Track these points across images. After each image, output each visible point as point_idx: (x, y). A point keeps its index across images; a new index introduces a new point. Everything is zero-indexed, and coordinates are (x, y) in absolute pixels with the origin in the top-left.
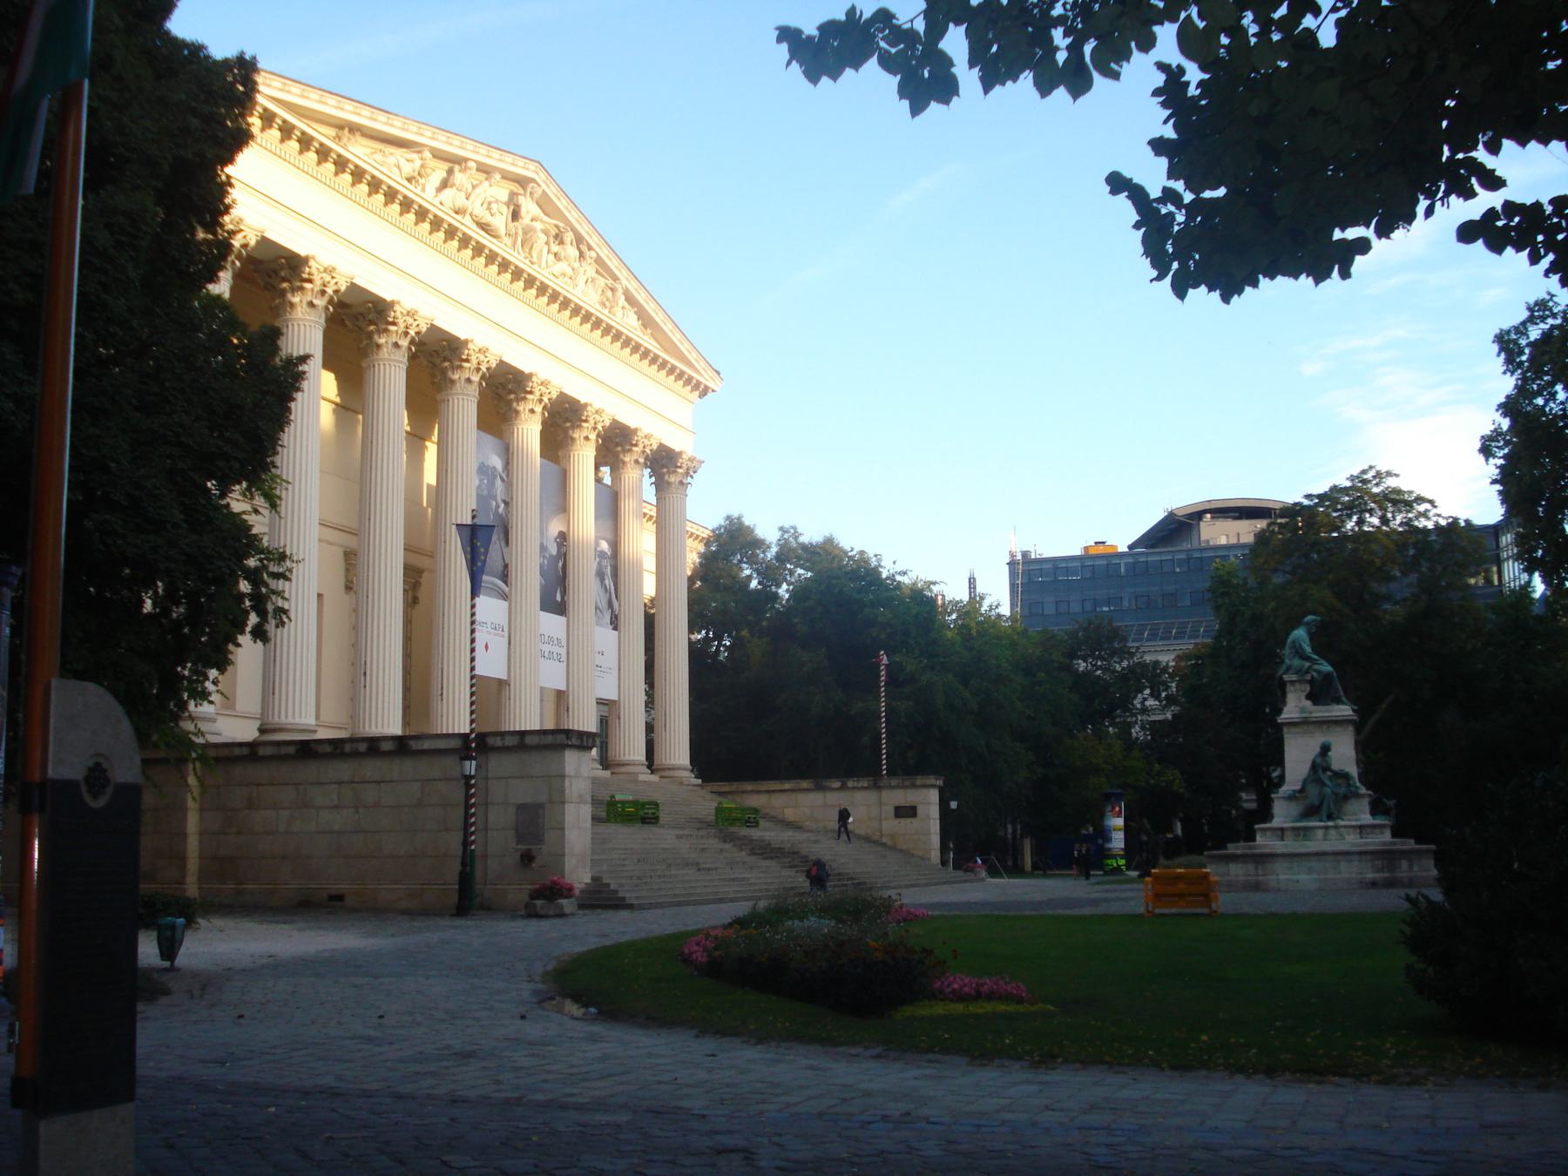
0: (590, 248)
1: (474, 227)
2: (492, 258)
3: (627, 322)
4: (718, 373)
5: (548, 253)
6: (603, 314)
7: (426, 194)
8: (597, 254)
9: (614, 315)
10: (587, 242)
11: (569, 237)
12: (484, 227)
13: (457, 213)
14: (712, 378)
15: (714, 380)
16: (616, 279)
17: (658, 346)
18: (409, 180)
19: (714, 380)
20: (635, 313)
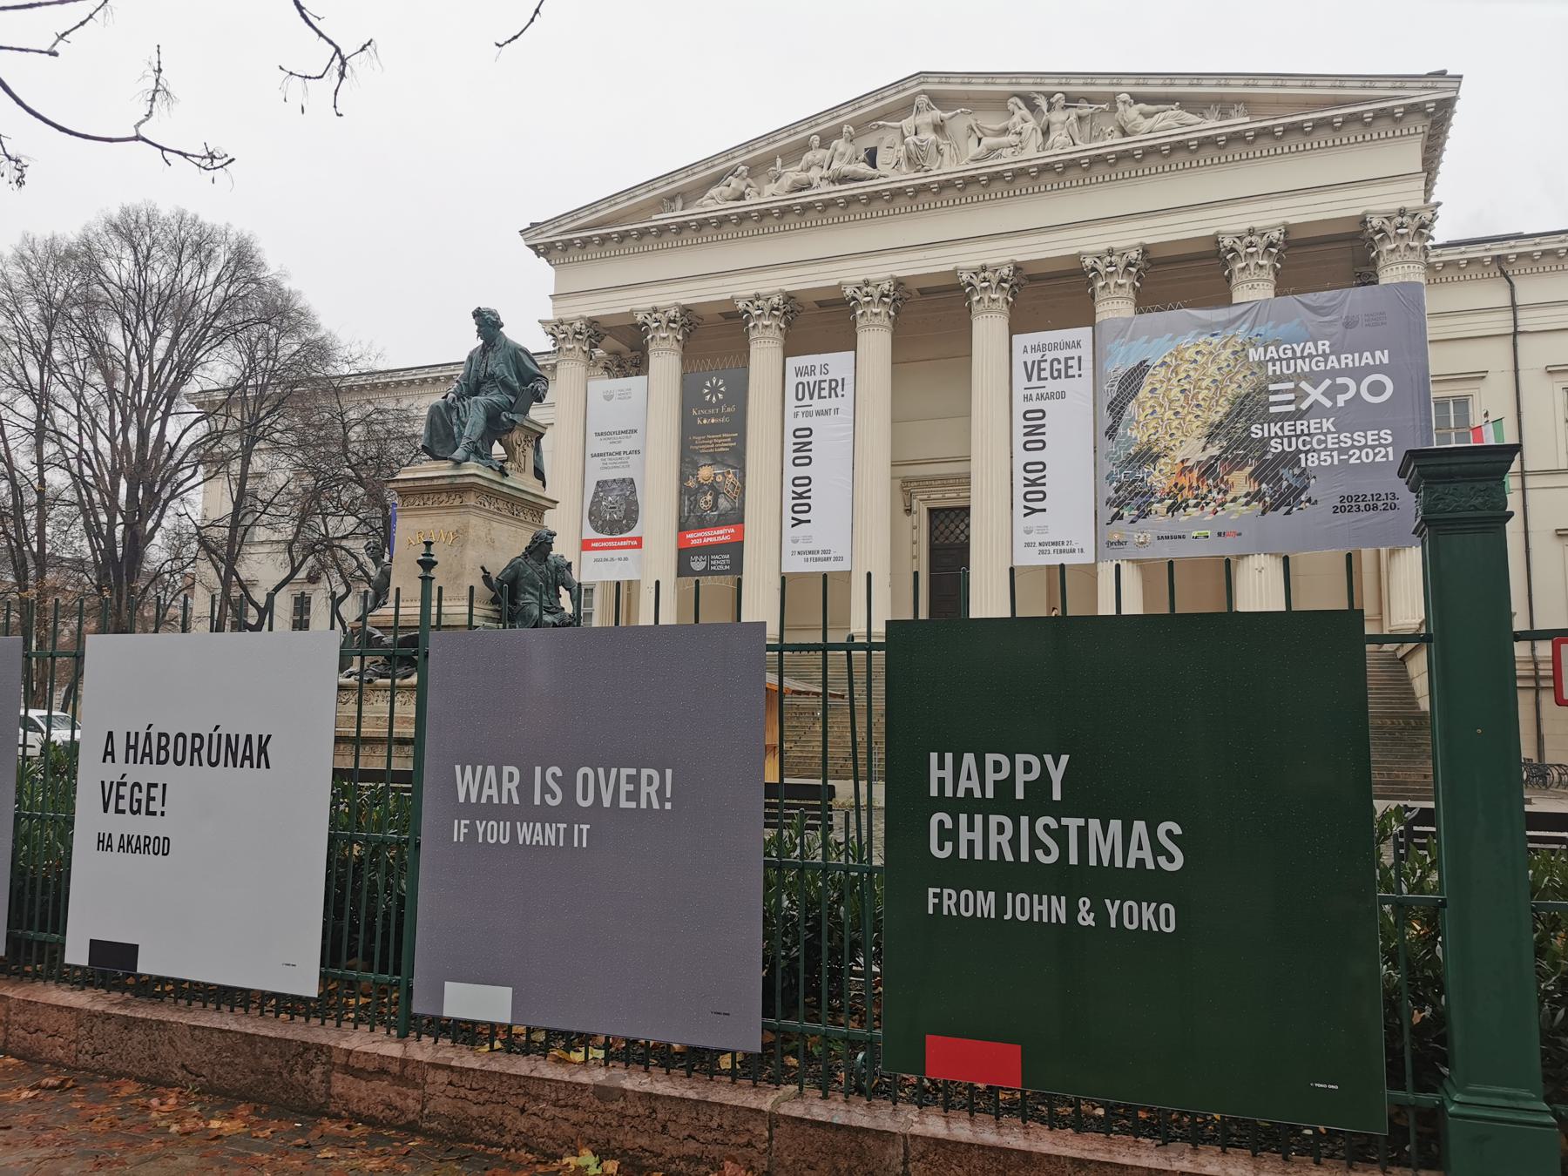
0: (1049, 95)
1: (832, 188)
2: (874, 197)
3: (1169, 124)
4: (1442, 74)
5: (980, 140)
6: (1112, 142)
7: (770, 193)
8: (1062, 93)
9: (1135, 133)
10: (1038, 92)
11: (1011, 107)
12: (843, 179)
13: (800, 190)
14: (1426, 88)
15: (1436, 88)
16: (1112, 99)
17: (1247, 119)
18: (741, 197)
19: (1436, 88)
20: (1181, 108)
